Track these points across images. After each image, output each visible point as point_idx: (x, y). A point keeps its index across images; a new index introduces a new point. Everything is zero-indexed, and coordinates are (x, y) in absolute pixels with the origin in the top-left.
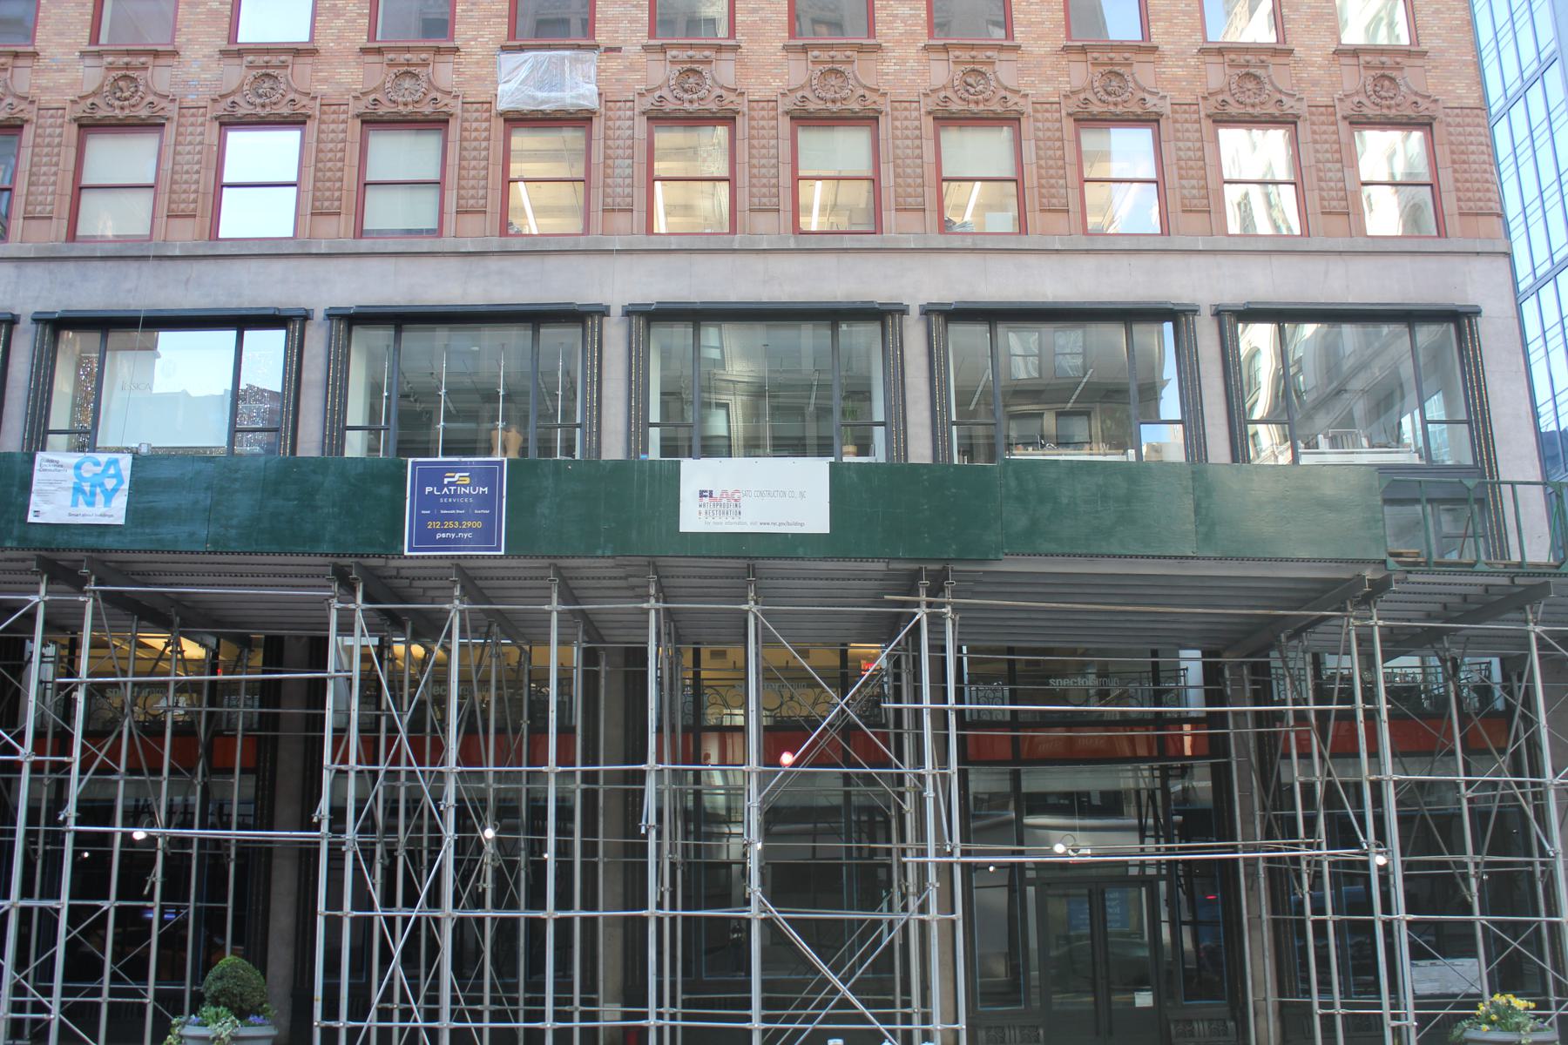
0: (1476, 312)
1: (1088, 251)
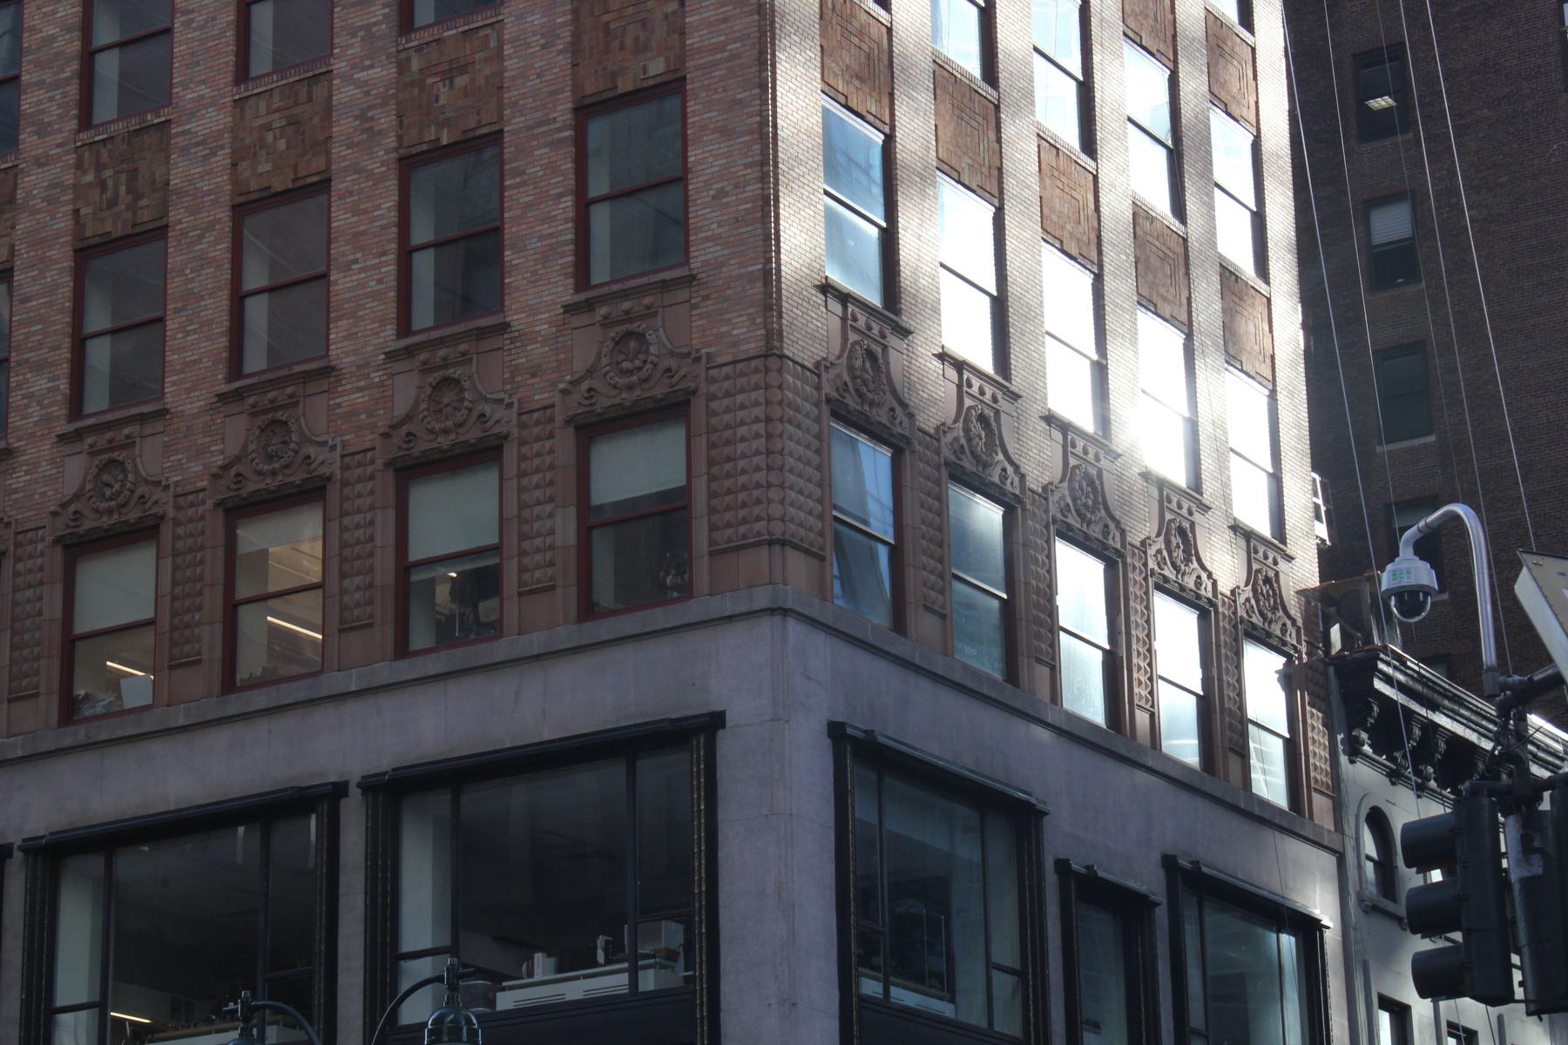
0: (715, 721)
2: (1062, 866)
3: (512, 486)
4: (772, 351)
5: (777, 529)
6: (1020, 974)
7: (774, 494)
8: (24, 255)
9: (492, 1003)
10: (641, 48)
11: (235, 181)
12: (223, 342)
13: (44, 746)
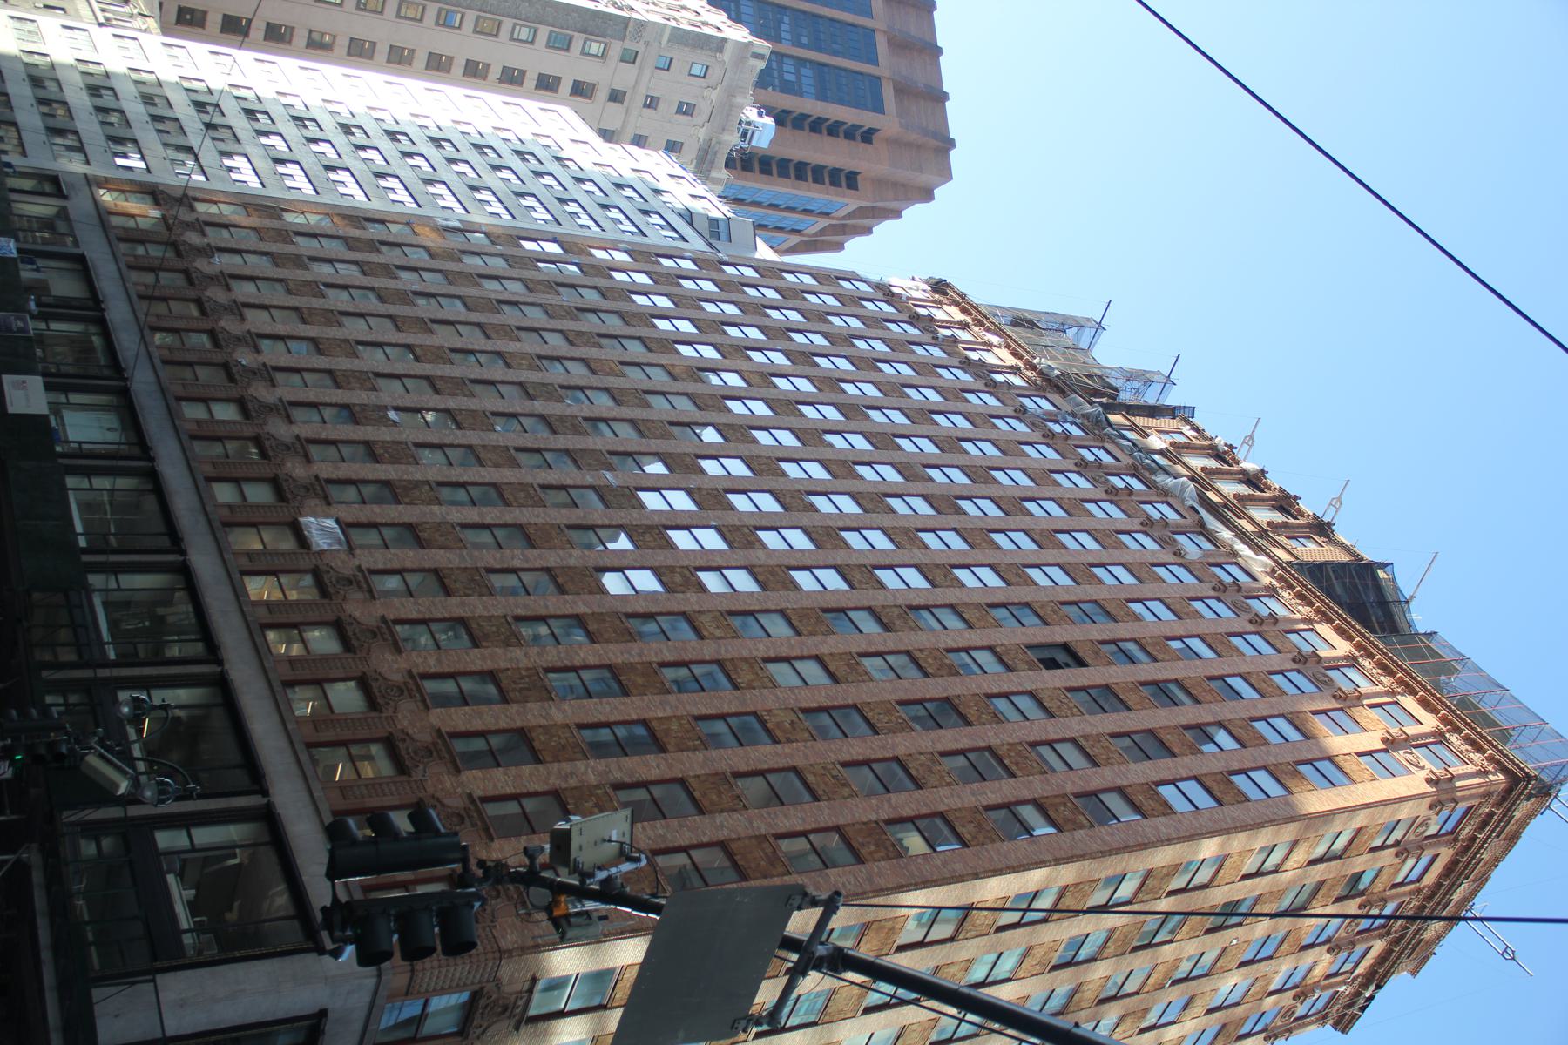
1: (291, 743)
4: (502, 953)
8: (487, 652)
11: (534, 727)
12: (463, 728)
13: (271, 676)
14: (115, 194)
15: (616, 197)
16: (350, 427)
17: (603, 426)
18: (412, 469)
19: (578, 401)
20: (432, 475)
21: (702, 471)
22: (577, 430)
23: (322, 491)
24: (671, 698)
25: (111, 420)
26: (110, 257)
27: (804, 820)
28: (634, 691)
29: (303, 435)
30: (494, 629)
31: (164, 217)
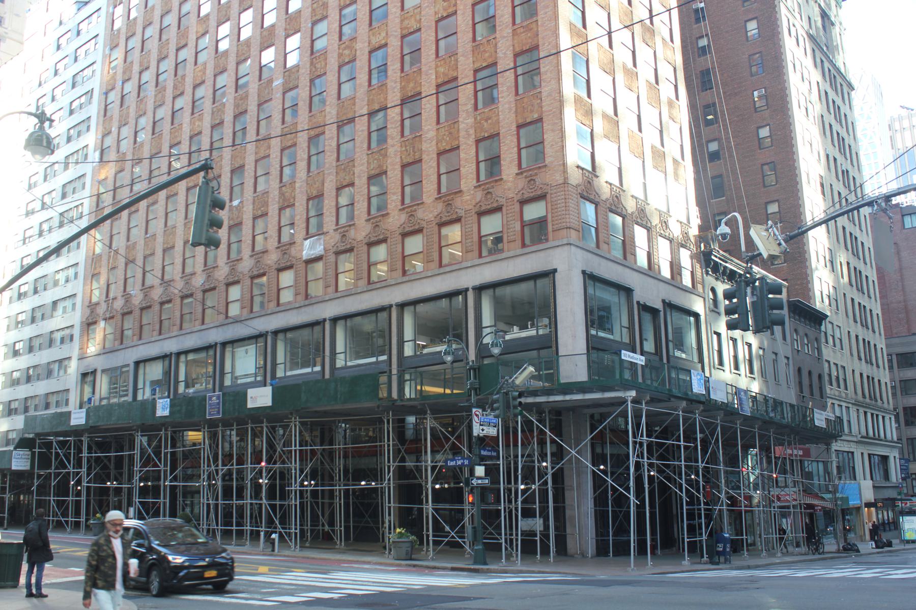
0: (555, 271)
1: (439, 274)
2: (638, 303)
3: (505, 217)
4: (566, 182)
5: (568, 225)
6: (629, 328)
7: (567, 216)
8: (389, 168)
9: (504, 338)
10: (532, 111)
11: (437, 148)
12: (436, 186)
14: (90, 345)
15: (69, 49)
16: (244, 227)
17: (241, 82)
18: (271, 196)
19: (224, 95)
20: (275, 184)
21: (273, 26)
22: (245, 97)
23: (284, 247)
24: (424, 69)
25: (240, 351)
26: (135, 349)
27: (505, 6)
28: (418, 89)
29: (250, 253)
30: (375, 162)
31: (105, 319)
